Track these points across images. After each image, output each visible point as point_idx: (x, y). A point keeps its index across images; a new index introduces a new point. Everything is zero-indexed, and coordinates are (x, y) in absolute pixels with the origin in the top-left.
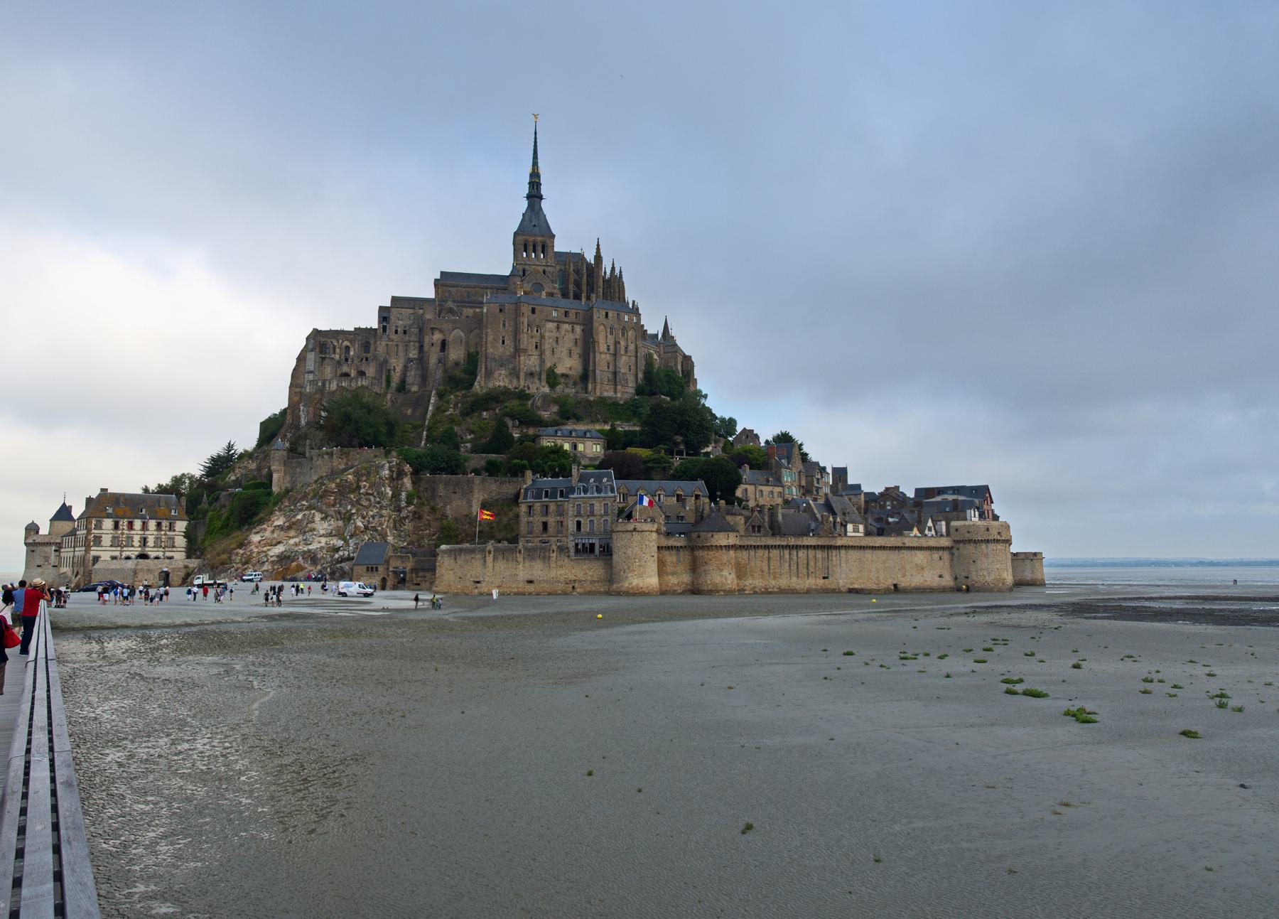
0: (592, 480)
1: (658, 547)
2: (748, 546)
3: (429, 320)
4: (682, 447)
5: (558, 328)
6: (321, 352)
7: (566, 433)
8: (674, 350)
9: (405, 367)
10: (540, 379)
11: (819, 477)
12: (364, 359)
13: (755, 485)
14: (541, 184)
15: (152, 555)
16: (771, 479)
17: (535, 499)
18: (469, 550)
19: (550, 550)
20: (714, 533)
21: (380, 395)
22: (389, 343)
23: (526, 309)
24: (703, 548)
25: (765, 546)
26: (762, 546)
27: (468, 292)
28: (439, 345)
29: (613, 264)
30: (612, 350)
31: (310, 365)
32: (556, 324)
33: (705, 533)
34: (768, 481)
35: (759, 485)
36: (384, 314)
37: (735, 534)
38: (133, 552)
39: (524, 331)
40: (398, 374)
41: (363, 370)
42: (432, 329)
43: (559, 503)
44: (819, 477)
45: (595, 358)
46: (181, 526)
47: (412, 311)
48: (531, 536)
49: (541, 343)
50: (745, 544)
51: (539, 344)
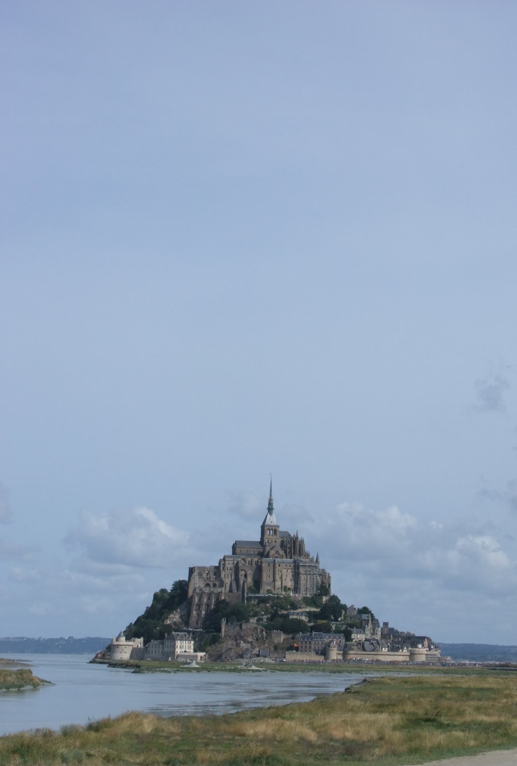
0: (318, 636)
1: (337, 654)
4: (333, 618)
5: (287, 571)
6: (199, 575)
7: (297, 614)
10: (282, 590)
11: (377, 629)
12: (214, 578)
13: (357, 634)
15: (187, 651)
23: (277, 565)
27: (248, 550)
30: (306, 579)
32: (286, 570)
34: (361, 632)
38: (183, 650)
44: (377, 629)
46: (192, 642)
47: (233, 562)
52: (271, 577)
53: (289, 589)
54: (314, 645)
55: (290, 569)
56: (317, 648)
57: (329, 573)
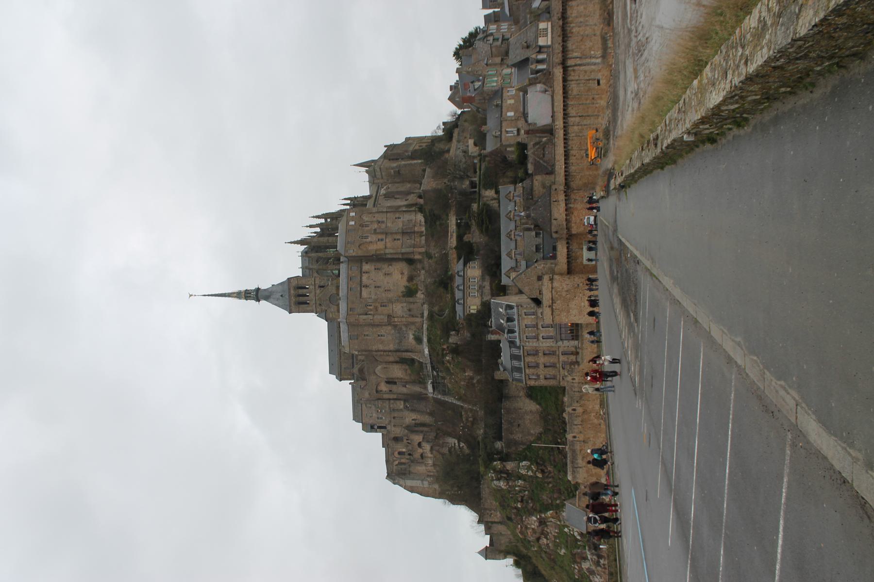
0: (502, 321)
1: (570, 272)
2: (566, 175)
3: (369, 394)
5: (366, 286)
6: (405, 474)
8: (378, 170)
9: (413, 410)
10: (414, 303)
11: (491, 38)
12: (408, 441)
13: (501, 121)
14: (246, 290)
16: (495, 104)
17: (522, 373)
18: (572, 455)
19: (573, 383)
20: (553, 218)
21: (437, 434)
22: (392, 424)
24: (568, 229)
25: (565, 155)
26: (565, 159)
28: (390, 385)
29: (307, 226)
30: (383, 237)
31: (416, 483)
32: (363, 289)
33: (553, 227)
34: (497, 106)
35: (501, 116)
36: (370, 428)
37: (553, 192)
39: (372, 318)
40: (419, 417)
41: (417, 443)
42: (377, 391)
43: (526, 354)
44: (491, 38)
45: (391, 254)
47: (364, 406)
48: (558, 376)
49: (382, 303)
50: (564, 178)
51: (383, 304)
52: (383, 331)
53: (411, 279)
54: (538, 340)
55: (361, 281)
56: (551, 332)
57: (385, 146)
